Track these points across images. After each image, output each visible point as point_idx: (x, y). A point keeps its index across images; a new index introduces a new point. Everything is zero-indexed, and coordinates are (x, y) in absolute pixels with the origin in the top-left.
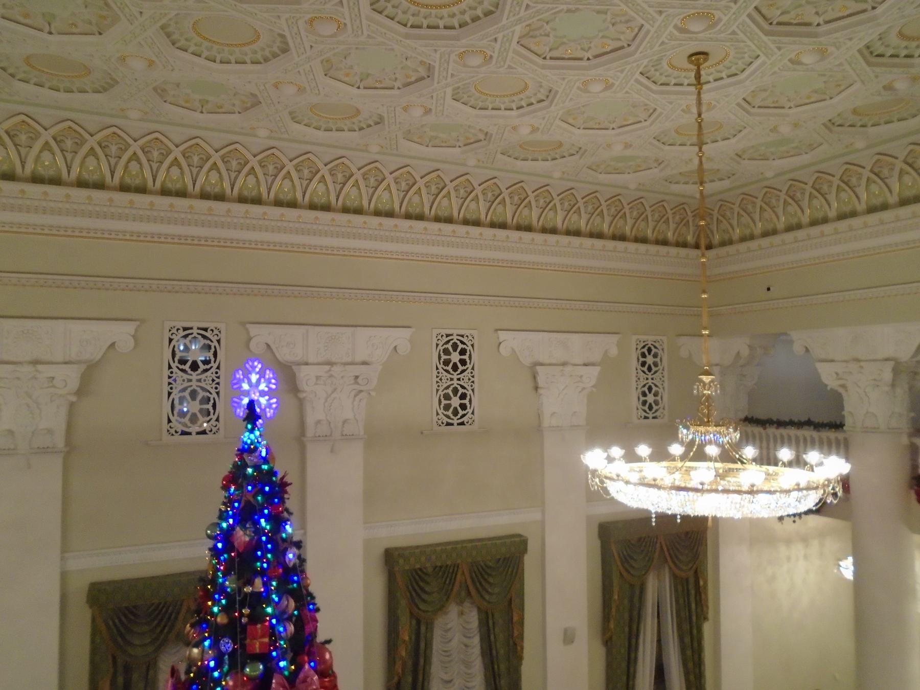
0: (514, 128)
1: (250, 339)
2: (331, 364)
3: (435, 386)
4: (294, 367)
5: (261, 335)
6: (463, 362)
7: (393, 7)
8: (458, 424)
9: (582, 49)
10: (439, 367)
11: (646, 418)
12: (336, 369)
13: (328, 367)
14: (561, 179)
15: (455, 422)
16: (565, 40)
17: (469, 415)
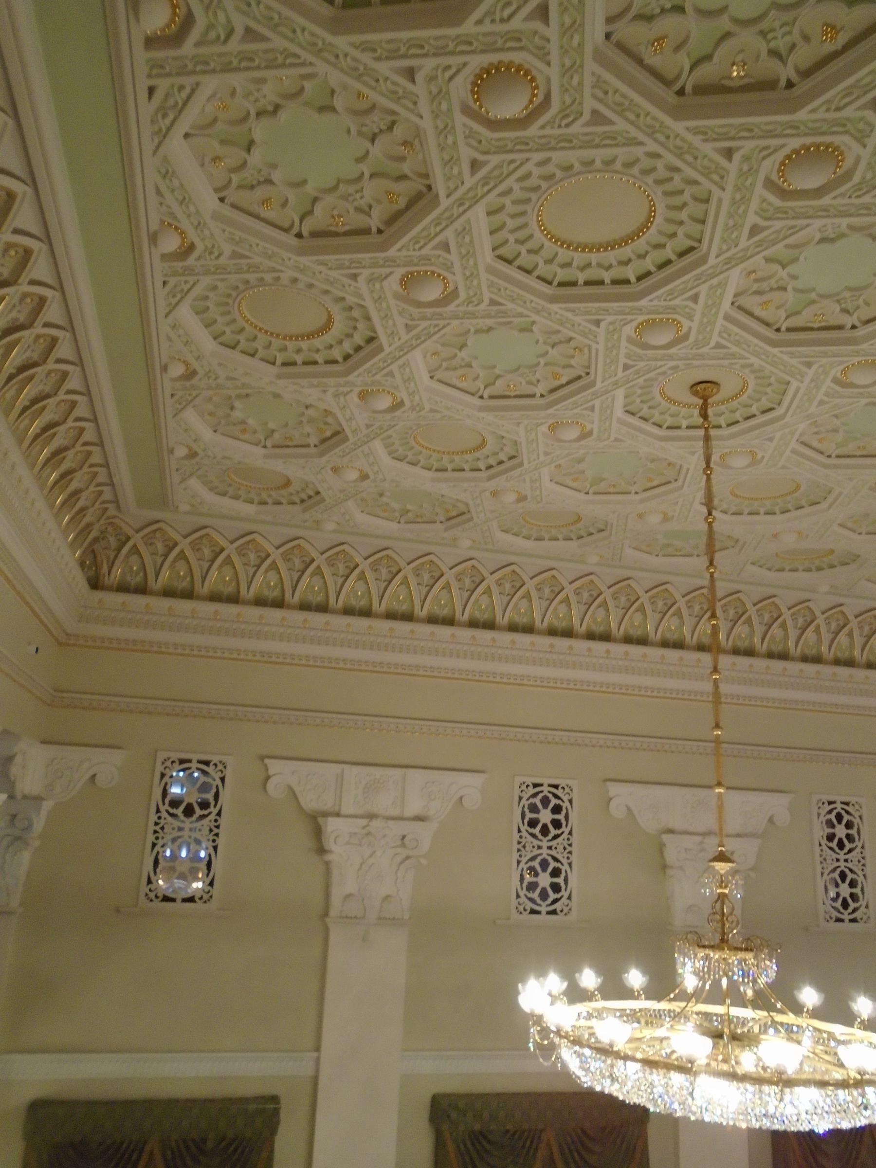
0: (640, 516)
1: (268, 778)
2: (372, 816)
3: (516, 856)
4: (320, 820)
5: (283, 774)
6: (557, 824)
7: (248, 340)
8: (548, 913)
9: (529, 383)
10: (523, 829)
11: (839, 920)
12: (376, 824)
13: (364, 822)
14: (334, 531)
15: (544, 909)
16: (497, 371)
17: (564, 900)
